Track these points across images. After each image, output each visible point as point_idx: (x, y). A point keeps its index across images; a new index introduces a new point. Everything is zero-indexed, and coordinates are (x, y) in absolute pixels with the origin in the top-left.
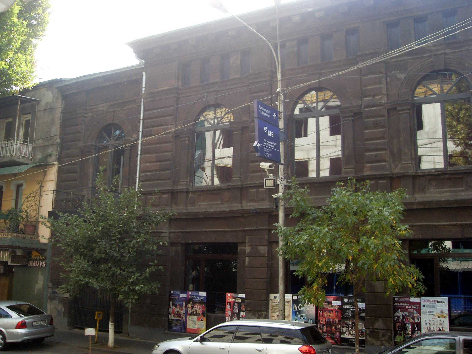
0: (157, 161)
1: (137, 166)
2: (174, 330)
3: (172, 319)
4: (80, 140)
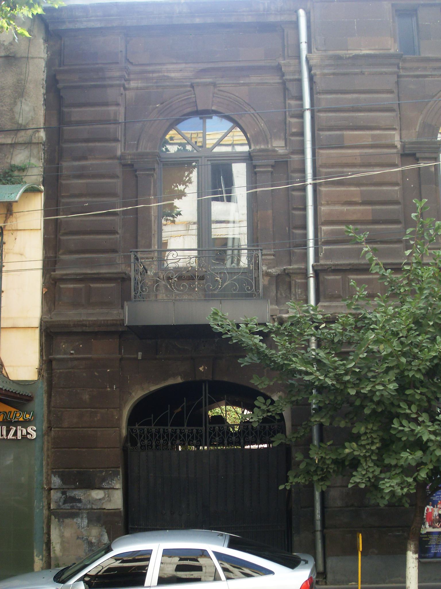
0: (364, 203)
1: (305, 209)
2: (435, 553)
3: (428, 533)
4: (116, 140)
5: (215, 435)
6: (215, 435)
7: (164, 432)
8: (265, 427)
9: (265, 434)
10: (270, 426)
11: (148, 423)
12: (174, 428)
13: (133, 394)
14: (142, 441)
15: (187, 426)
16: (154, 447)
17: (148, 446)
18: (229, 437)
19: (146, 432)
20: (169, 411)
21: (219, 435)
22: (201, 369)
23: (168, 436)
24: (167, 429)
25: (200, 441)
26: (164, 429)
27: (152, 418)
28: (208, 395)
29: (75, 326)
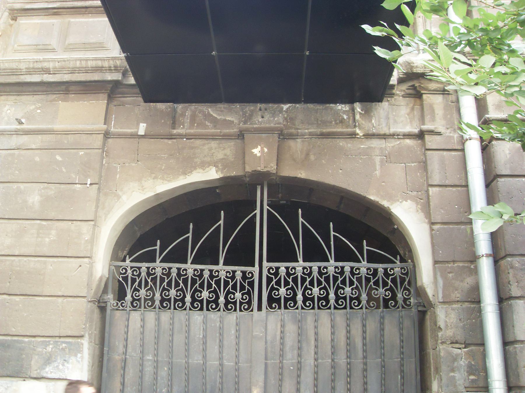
5: (278, 283)
6: (278, 283)
7: (179, 275)
8: (376, 271)
9: (376, 283)
10: (386, 270)
11: (150, 257)
12: (199, 267)
13: (124, 197)
14: (136, 290)
15: (224, 264)
16: (157, 303)
17: (146, 300)
18: (306, 288)
19: (144, 274)
20: (190, 235)
21: (287, 283)
22: (257, 151)
23: (185, 282)
24: (186, 270)
25: (248, 293)
26: (179, 269)
27: (158, 247)
28: (266, 207)
29: (29, 72)
